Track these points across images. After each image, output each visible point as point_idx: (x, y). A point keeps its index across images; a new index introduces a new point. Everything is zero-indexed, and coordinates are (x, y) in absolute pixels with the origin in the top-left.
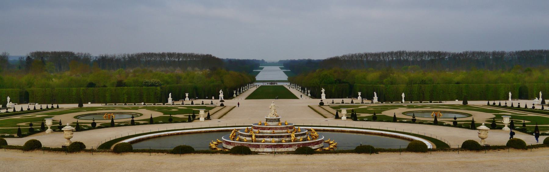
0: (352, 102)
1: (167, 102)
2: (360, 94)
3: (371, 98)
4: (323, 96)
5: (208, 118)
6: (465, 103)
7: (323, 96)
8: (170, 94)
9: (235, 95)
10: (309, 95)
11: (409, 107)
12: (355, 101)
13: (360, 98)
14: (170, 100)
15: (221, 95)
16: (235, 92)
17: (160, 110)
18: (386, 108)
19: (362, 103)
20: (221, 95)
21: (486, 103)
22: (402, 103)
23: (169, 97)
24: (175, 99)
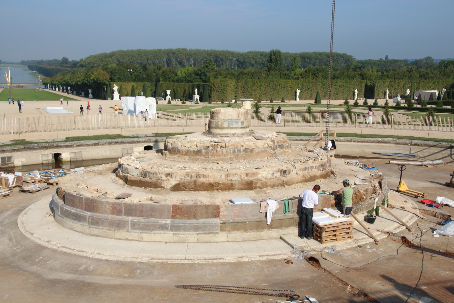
2: (169, 92)
10: (91, 95)
21: (342, 102)
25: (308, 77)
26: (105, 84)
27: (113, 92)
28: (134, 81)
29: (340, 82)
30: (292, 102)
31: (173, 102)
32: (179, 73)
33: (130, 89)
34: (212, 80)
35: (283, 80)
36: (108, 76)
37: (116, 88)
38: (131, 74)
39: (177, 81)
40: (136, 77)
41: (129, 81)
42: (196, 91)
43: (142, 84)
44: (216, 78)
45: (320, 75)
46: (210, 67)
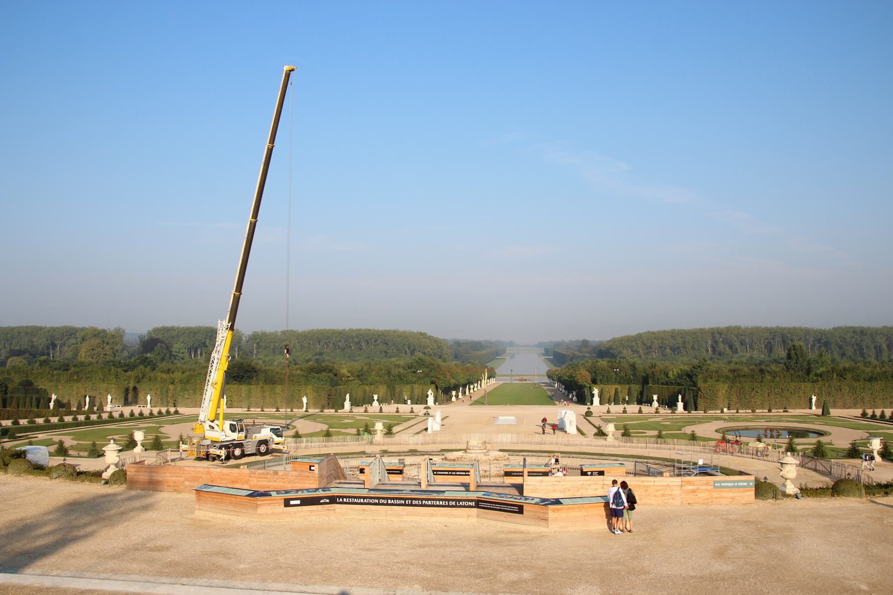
0: (640, 411)
1: (343, 407)
2: (655, 397)
3: (671, 404)
4: (596, 400)
5: (389, 432)
6: (825, 413)
7: (596, 400)
8: (348, 396)
9: (454, 399)
11: (732, 419)
12: (645, 409)
13: (655, 404)
14: (347, 404)
15: (431, 400)
16: (454, 393)
17: (325, 420)
18: (693, 422)
19: (657, 412)
20: (431, 400)
21: (858, 412)
22: (722, 412)
23: (345, 400)
24: (355, 403)
25: (832, 379)
26: (585, 386)
27: (593, 396)
28: (619, 383)
29: (877, 385)
30: (808, 411)
31: (661, 410)
32: (670, 374)
33: (613, 393)
34: (700, 384)
35: (792, 385)
36: (589, 377)
37: (596, 392)
38: (616, 374)
39: (667, 384)
40: (622, 378)
41: (613, 384)
42: (680, 397)
43: (627, 386)
44: (705, 381)
45: (849, 376)
46: (704, 367)
